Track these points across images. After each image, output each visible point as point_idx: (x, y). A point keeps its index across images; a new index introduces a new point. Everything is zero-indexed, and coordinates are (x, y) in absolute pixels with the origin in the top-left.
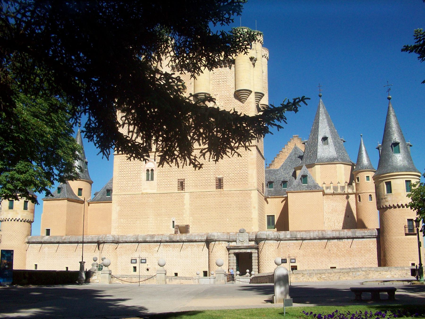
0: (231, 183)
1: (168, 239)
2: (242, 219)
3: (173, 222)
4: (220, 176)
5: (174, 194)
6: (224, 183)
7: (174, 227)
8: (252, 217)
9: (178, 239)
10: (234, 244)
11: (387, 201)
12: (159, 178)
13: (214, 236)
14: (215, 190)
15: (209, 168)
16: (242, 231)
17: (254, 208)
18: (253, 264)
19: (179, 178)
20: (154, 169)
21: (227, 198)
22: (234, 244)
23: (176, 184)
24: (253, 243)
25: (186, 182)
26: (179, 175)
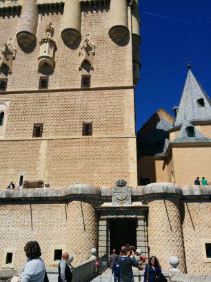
0: (102, 129)
1: (4, 196)
3: (22, 177)
4: (89, 121)
5: (27, 142)
6: (94, 129)
8: (130, 171)
9: (20, 196)
10: (106, 204)
12: (9, 123)
13: (77, 189)
14: (81, 136)
15: (75, 112)
16: (122, 184)
17: (132, 159)
18: (138, 238)
19: (36, 122)
20: (5, 112)
22: (106, 204)
23: (31, 130)
24: (139, 204)
25: (44, 127)
26: (36, 119)
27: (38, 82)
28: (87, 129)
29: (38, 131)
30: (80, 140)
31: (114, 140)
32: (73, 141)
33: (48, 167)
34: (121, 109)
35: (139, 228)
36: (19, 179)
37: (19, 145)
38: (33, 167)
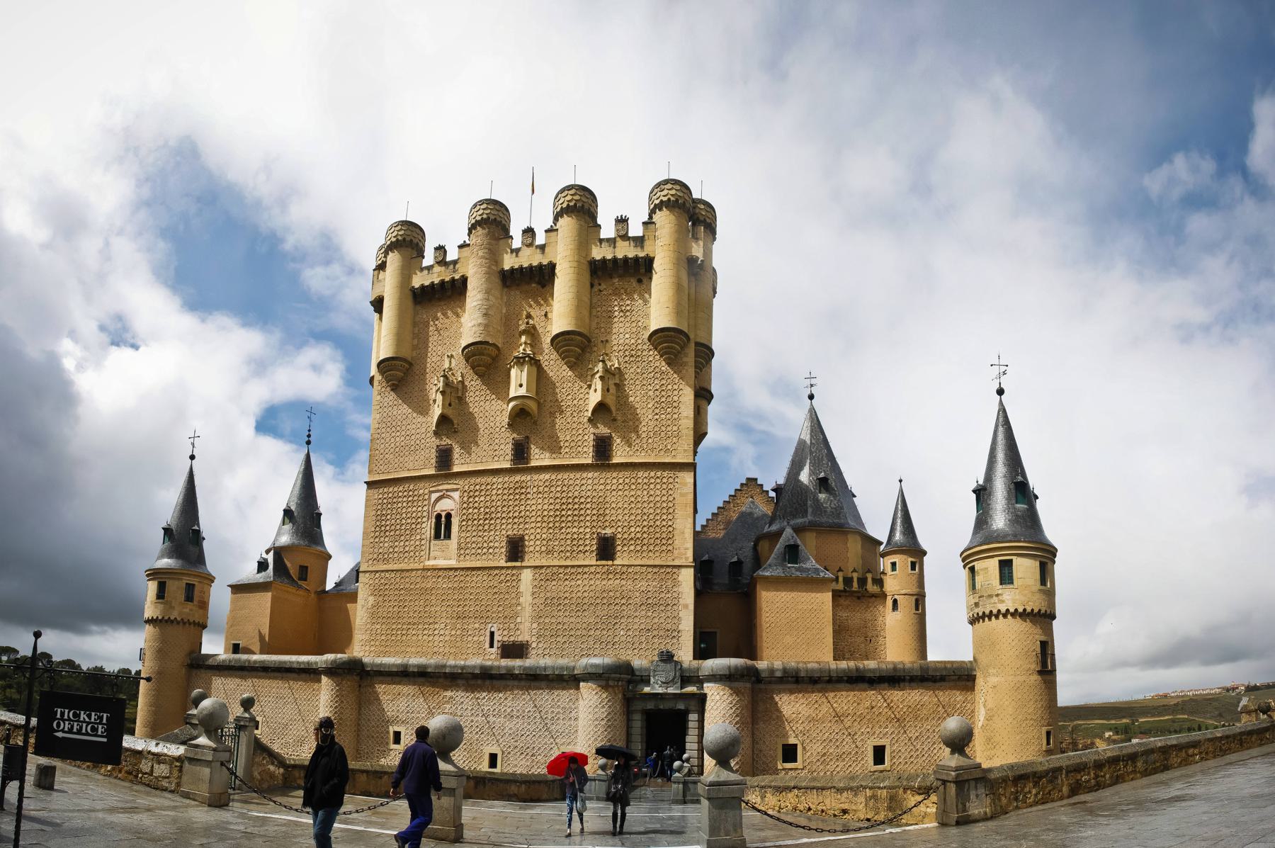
2: (655, 633)
3: (492, 634)
4: (608, 531)
6: (619, 548)
7: (492, 646)
8: (681, 627)
11: (1003, 601)
14: (594, 562)
17: (686, 606)
18: (688, 739)
21: (624, 582)
24: (691, 689)
27: (508, 449)
28: (606, 549)
29: (516, 549)
30: (592, 569)
31: (655, 570)
32: (580, 570)
33: (537, 617)
34: (670, 511)
35: (691, 724)
36: (488, 639)
37: (482, 576)
38: (510, 617)
